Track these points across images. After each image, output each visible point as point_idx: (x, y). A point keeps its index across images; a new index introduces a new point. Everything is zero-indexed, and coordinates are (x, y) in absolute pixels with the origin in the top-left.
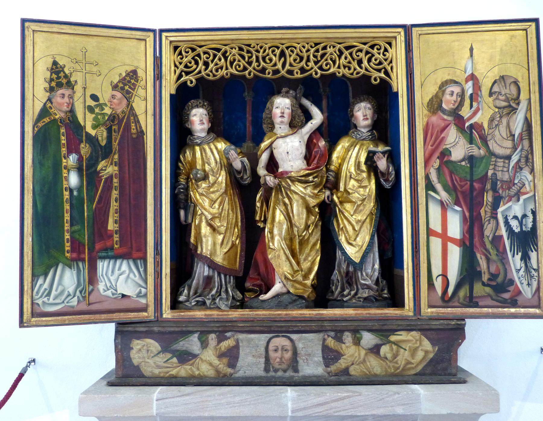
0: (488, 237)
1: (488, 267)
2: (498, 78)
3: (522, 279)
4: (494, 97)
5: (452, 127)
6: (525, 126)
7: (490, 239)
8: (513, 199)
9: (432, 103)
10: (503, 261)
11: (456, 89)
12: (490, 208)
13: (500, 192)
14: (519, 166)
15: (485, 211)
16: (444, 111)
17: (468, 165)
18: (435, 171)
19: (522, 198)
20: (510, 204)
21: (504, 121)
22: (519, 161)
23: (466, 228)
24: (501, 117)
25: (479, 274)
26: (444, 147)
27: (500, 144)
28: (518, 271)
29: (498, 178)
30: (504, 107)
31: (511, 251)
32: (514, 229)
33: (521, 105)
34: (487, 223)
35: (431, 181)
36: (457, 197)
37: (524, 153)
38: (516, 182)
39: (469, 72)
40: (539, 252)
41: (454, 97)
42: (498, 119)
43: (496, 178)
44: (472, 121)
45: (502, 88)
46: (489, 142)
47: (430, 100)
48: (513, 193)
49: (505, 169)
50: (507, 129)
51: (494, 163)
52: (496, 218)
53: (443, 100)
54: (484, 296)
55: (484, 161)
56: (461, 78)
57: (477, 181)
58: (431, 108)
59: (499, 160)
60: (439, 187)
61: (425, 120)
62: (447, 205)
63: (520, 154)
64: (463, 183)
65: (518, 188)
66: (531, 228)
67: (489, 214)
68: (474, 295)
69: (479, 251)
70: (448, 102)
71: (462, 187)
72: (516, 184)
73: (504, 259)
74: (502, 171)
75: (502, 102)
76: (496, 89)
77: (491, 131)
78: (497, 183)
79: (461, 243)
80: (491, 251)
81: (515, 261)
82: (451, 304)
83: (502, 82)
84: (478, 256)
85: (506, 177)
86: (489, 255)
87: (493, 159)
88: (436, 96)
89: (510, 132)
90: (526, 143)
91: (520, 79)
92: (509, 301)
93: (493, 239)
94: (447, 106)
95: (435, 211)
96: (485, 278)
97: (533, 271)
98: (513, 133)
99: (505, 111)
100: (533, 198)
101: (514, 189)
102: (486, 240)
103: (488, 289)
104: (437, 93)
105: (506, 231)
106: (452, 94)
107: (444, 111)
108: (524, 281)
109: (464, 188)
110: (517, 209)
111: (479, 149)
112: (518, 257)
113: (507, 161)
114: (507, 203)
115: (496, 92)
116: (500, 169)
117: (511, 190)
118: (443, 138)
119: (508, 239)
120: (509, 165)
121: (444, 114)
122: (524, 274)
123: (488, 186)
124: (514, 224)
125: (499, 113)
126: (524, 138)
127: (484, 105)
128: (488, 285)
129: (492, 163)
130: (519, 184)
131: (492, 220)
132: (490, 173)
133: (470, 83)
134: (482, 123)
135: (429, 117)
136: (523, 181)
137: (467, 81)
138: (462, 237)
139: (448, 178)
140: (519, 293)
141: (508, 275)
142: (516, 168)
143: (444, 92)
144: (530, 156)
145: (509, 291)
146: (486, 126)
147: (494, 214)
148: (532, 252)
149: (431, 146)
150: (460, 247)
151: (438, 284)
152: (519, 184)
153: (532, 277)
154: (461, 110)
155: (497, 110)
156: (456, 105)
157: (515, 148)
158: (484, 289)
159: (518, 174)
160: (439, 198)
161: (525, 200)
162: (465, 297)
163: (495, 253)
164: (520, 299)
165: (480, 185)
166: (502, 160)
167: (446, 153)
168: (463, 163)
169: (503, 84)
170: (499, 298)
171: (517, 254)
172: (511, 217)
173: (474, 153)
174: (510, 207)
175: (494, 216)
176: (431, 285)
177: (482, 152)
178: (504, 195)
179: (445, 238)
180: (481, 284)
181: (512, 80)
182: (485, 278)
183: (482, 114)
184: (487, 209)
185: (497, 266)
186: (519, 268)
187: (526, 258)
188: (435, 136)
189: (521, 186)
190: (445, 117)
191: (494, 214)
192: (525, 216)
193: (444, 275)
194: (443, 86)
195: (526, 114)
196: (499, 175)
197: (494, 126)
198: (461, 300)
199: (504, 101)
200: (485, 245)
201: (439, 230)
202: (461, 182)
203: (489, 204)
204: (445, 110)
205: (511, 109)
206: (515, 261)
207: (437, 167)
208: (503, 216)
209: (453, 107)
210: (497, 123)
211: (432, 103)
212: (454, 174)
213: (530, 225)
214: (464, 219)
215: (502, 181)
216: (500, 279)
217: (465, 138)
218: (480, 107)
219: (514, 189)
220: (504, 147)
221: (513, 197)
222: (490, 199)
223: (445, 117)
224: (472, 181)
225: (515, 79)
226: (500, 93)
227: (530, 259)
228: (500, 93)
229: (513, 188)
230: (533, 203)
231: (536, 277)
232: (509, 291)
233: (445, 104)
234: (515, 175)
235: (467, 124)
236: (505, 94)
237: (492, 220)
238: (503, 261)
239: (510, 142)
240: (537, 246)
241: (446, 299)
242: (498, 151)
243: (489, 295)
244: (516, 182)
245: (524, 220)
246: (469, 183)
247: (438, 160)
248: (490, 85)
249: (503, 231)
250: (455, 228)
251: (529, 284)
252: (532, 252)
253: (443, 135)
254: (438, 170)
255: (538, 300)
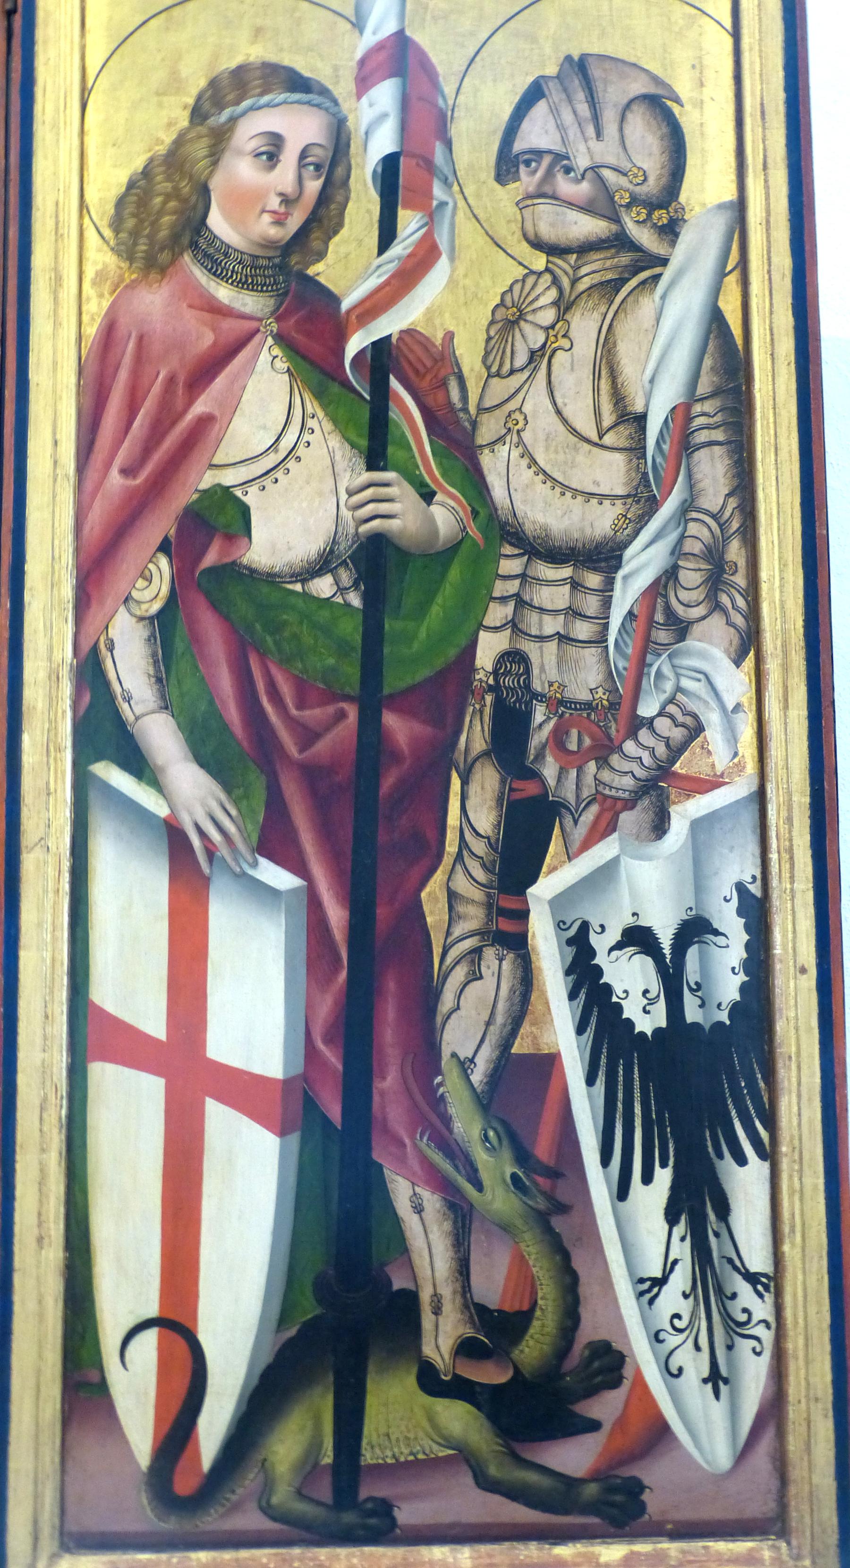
0: (465, 1066)
1: (463, 1269)
2: (551, 70)
3: (673, 1340)
4: (528, 180)
5: (264, 357)
6: (708, 362)
7: (477, 1077)
8: (626, 818)
9: (143, 202)
10: (558, 1223)
11: (302, 128)
12: (480, 875)
13: (549, 770)
14: (669, 612)
15: (452, 896)
16: (216, 259)
17: (355, 600)
18: (141, 632)
19: (685, 813)
20: (605, 851)
21: (585, 326)
22: (670, 575)
23: (326, 1006)
24: (564, 306)
25: (401, 1315)
26: (208, 480)
27: (552, 471)
28: (650, 1288)
29: (537, 686)
30: (585, 248)
31: (605, 1160)
32: (632, 1010)
33: (687, 237)
34: (459, 974)
35: (112, 698)
36: (276, 807)
37: (700, 531)
38: (648, 708)
39: (381, 23)
40: (785, 1165)
41: (285, 175)
42: (548, 316)
43: (528, 686)
44: (388, 325)
45: (573, 132)
46: (486, 459)
47: (131, 185)
48: (628, 782)
49: (583, 630)
50: (596, 376)
51: (513, 587)
52: (517, 943)
53: (216, 184)
54: (434, 1464)
55: (454, 573)
56: (330, 59)
57: (401, 702)
58: (135, 234)
59: (545, 571)
60: (161, 736)
61: (97, 307)
62: (210, 853)
63: (672, 537)
64: (314, 715)
65: (661, 750)
66: (735, 1009)
67: (473, 918)
68: (368, 1457)
69: (401, 1160)
70: (244, 201)
71: (308, 736)
72: (649, 723)
73: (563, 1209)
74: (564, 639)
75: (573, 215)
76: (537, 132)
77: (499, 389)
78: (528, 716)
79: (288, 1106)
80: (481, 1156)
81: (634, 1227)
82: (212, 1521)
83: (580, 95)
84: (401, 1190)
85: (585, 679)
86: (469, 1189)
87: (511, 566)
88: (173, 160)
89: (618, 398)
90: (713, 471)
91: (683, 86)
92: (592, 1490)
93: (495, 1077)
94: (237, 223)
95: (130, 893)
96: (442, 1336)
97: (744, 1289)
98: (639, 407)
99: (595, 269)
100: (749, 818)
101: (636, 756)
102: (451, 1086)
103: (457, 1418)
104: (180, 141)
105: (580, 1030)
106: (272, 150)
107: (216, 259)
108: (684, 1357)
109: (322, 747)
110: (649, 884)
111: (428, 496)
112: (652, 1196)
113: (594, 580)
114: (587, 844)
115: (539, 154)
116: (551, 625)
117: (615, 760)
118: (205, 422)
119: (590, 1081)
120: (607, 604)
121: (218, 272)
122: (685, 1307)
123: (475, 735)
124: (631, 980)
125: (556, 281)
126: (702, 437)
127: (467, 230)
128: (459, 1389)
129: (500, 588)
130: (663, 725)
131: (490, 954)
132: (489, 649)
133: (385, 94)
134: (450, 336)
135: (123, 292)
136: (693, 706)
137: (364, 82)
138: (299, 1068)
139: (225, 683)
140: (659, 1433)
141: (585, 1314)
142: (651, 623)
143: (220, 140)
144: (735, 552)
145: (594, 1426)
146: (469, 355)
147: (503, 912)
148: (741, 1160)
149: (126, 472)
150: (282, 1133)
151: (135, 1383)
152: (663, 725)
153: (736, 1328)
154: (321, 255)
155: (539, 261)
156: (295, 222)
157: (643, 500)
158: (431, 1419)
159: (661, 663)
160: (163, 811)
161: (697, 826)
162: (308, 1469)
163: (509, 1169)
164: (657, 1477)
165: (419, 729)
166: (566, 572)
167: (221, 517)
168: (323, 586)
169: (584, 109)
170: (532, 1477)
171: (647, 1178)
172: (614, 935)
173: (394, 524)
174: (607, 872)
175: (508, 934)
176: (84, 1388)
177: (445, 517)
178: (569, 794)
179: (188, 1072)
180: (411, 1381)
181: (639, 87)
182: (442, 1336)
183: (452, 283)
184: (461, 884)
185: (520, 1261)
186: (658, 1274)
187: (698, 1203)
188: (153, 408)
189: (677, 734)
190: (224, 293)
191: (503, 912)
192: (695, 929)
193: (176, 1326)
194: (220, 106)
195: (716, 290)
196: (545, 661)
197: (521, 359)
198: (282, 1495)
199: (588, 208)
200: (447, 1120)
201: (153, 1021)
202: (300, 706)
203: (479, 847)
204: (227, 250)
205: (625, 259)
206: (634, 1227)
207: (156, 607)
208: (560, 925)
209: (273, 232)
210: (537, 339)
211: (143, 202)
212: (263, 657)
213: (729, 987)
214: (315, 950)
215: (559, 704)
216: (533, 1348)
217: (341, 425)
218: (443, 243)
219: (636, 756)
220: (576, 492)
221: (630, 804)
222: (485, 819)
223: (224, 293)
224: (371, 701)
225: (656, 80)
226: (561, 161)
227: (723, 1210)
228: (561, 161)
229: (629, 747)
230: (753, 848)
231: (760, 1331)
232: (594, 1426)
233: (227, 215)
234: (641, 666)
235: (355, 344)
236: (594, 169)
237: (490, 954)
238: (558, 1223)
239: (619, 459)
240: (771, 1121)
241: (184, 1484)
242: (543, 511)
243: (463, 1456)
244: (648, 708)
245: (692, 954)
246: (353, 713)
247: (163, 562)
248: (507, 111)
249: (561, 1031)
250: (255, 1012)
251: (715, 1378)
252: (741, 1160)
253: (200, 407)
254: (164, 626)
255: (774, 1484)
